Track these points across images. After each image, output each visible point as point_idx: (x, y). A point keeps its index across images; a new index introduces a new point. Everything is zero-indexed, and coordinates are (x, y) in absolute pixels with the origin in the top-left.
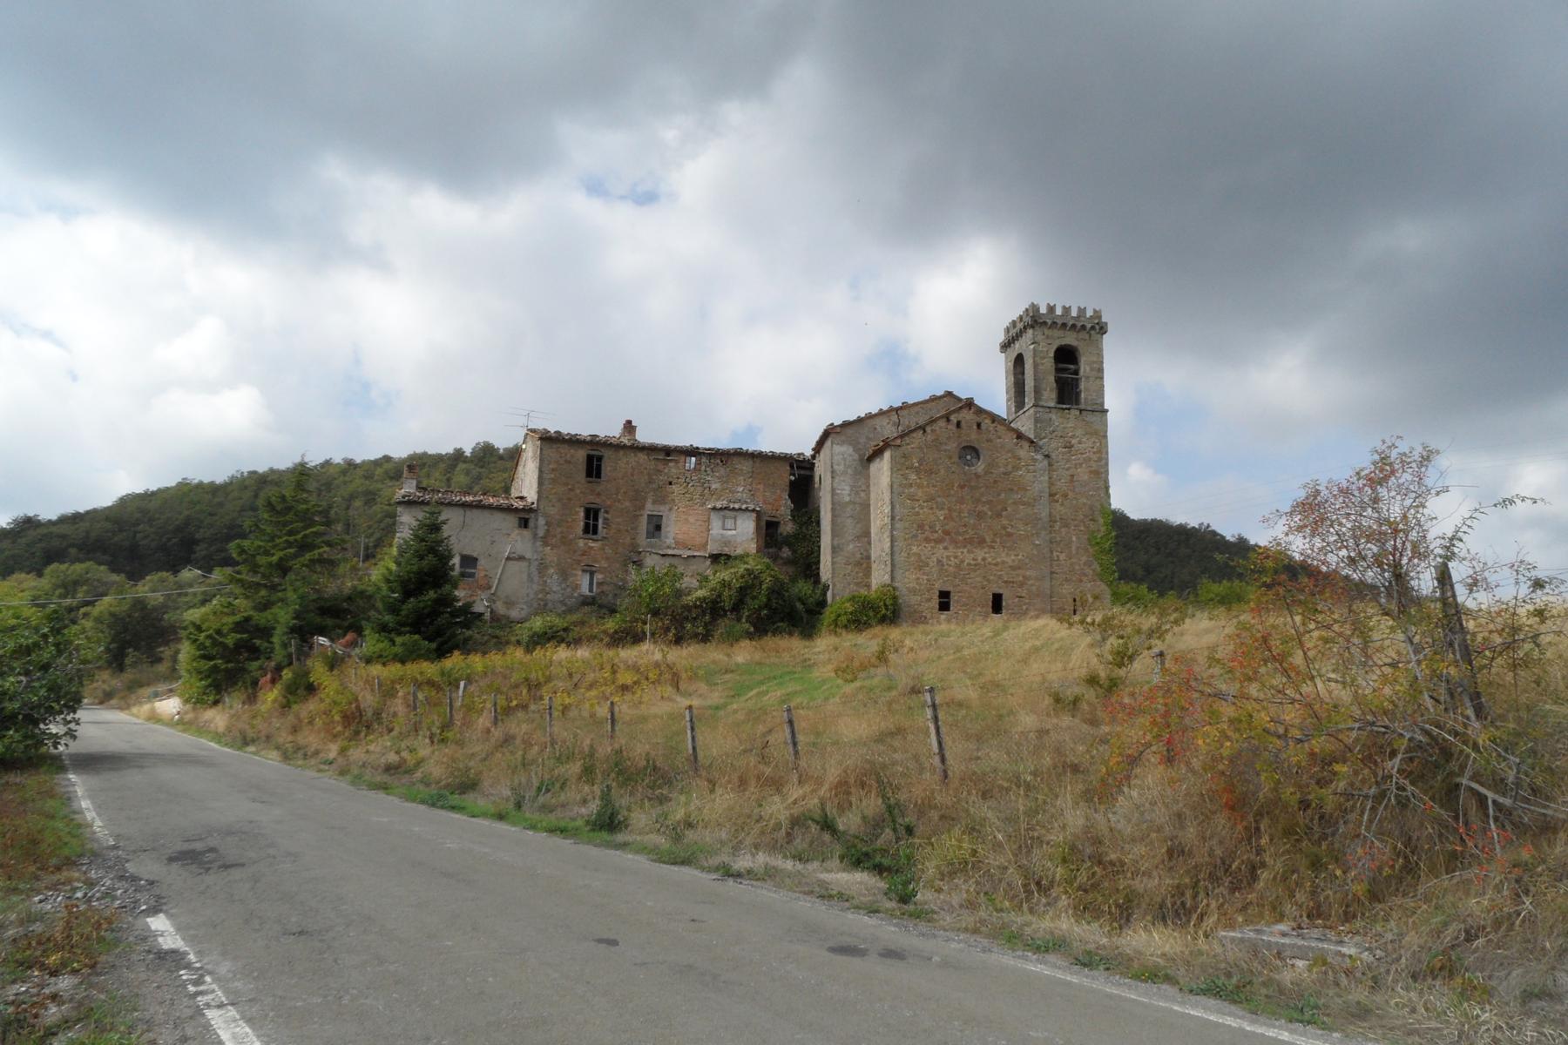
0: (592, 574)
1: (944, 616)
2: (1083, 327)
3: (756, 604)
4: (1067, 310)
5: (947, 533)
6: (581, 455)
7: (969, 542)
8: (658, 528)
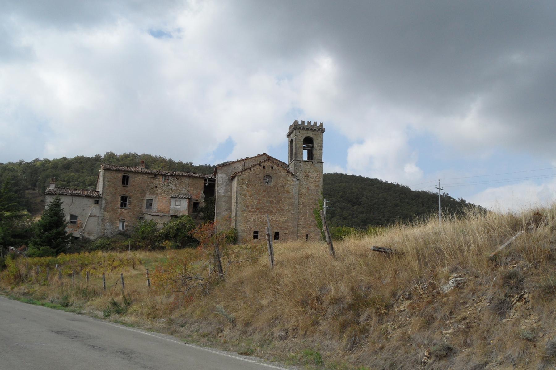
0: (124, 222)
1: (255, 240)
2: (315, 130)
3: (183, 235)
4: (309, 123)
5: (258, 209)
6: (120, 175)
7: (266, 212)
8: (151, 205)
